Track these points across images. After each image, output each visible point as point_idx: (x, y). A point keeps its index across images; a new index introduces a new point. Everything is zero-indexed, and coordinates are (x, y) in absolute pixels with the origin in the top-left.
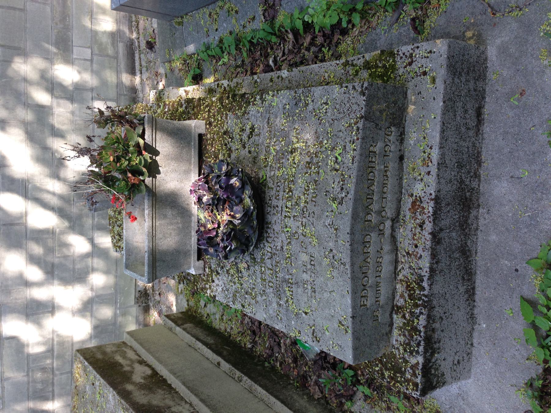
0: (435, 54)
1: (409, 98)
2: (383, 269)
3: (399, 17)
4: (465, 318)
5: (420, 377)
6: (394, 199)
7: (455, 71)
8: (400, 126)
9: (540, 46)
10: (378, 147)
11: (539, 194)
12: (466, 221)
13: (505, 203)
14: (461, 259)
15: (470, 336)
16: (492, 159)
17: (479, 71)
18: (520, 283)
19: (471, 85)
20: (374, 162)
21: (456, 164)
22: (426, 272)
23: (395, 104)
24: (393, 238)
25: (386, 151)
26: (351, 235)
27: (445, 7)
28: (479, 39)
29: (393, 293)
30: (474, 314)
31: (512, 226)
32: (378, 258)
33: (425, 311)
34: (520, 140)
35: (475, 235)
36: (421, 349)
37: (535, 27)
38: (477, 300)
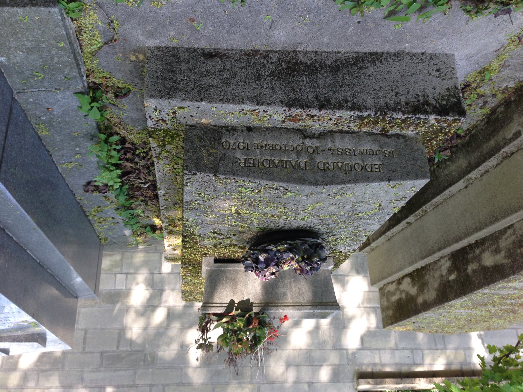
0: (158, 107)
1: (195, 122)
2: (348, 147)
3: (112, 104)
4: (398, 64)
5: (448, 118)
6: (286, 136)
7: (173, 89)
8: (221, 132)
9: (148, 7)
10: (241, 156)
11: (289, 6)
12: (309, 67)
13: (295, 31)
14: (344, 72)
15: (415, 56)
16: (252, 41)
17: (170, 57)
18: (372, 19)
19: (184, 66)
20: (254, 160)
21: (257, 82)
22: (354, 113)
23: (202, 139)
24: (321, 136)
25: (244, 148)
26: (318, 185)
27: (105, 73)
28: (139, 52)
29: (370, 135)
30: (395, 53)
31: (316, 27)
32: (338, 153)
33: (389, 114)
34: (236, 22)
35: (321, 54)
36: (422, 117)
37: (129, 10)
38: (382, 51)
